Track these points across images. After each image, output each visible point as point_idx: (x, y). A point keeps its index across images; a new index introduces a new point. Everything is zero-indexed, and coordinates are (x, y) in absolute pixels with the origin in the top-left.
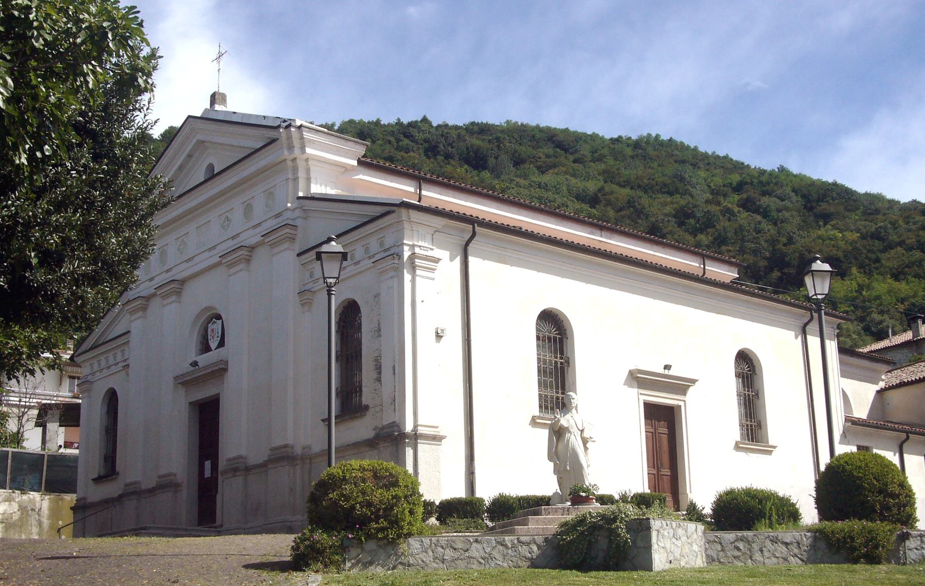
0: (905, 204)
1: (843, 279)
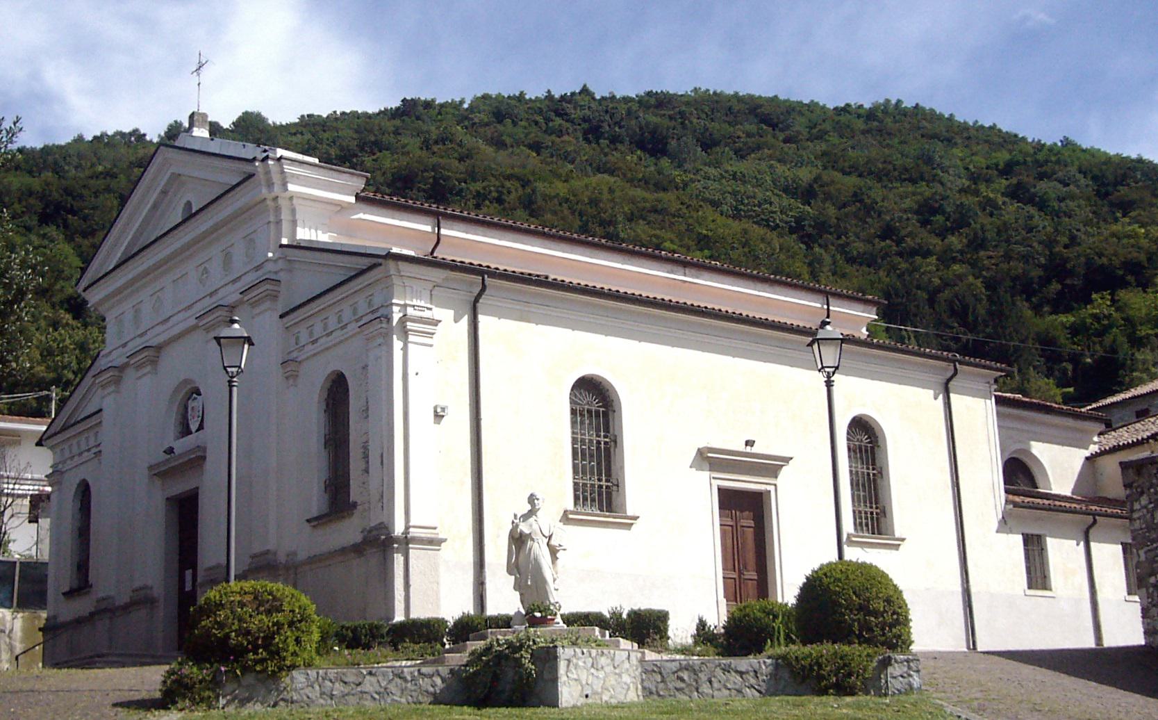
1: (1145, 292)
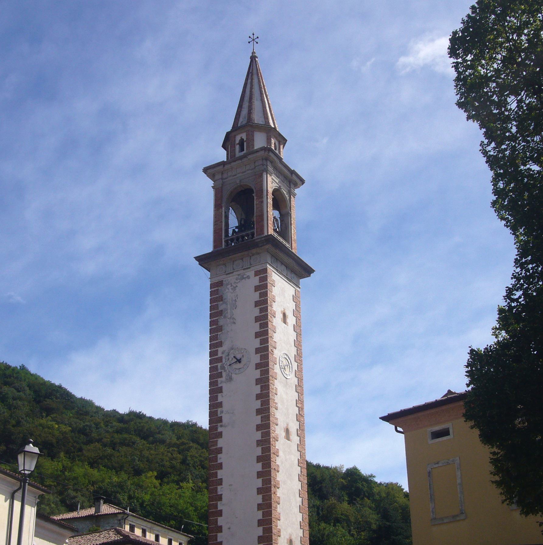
0: (107, 411)
1: (52, 460)
